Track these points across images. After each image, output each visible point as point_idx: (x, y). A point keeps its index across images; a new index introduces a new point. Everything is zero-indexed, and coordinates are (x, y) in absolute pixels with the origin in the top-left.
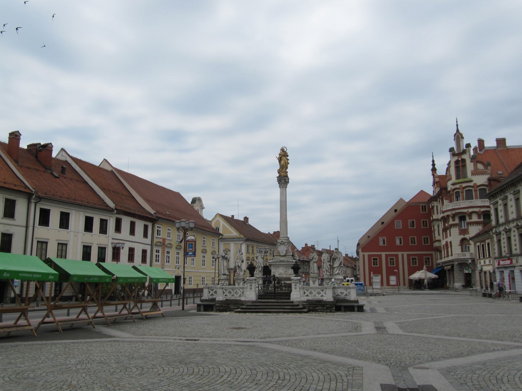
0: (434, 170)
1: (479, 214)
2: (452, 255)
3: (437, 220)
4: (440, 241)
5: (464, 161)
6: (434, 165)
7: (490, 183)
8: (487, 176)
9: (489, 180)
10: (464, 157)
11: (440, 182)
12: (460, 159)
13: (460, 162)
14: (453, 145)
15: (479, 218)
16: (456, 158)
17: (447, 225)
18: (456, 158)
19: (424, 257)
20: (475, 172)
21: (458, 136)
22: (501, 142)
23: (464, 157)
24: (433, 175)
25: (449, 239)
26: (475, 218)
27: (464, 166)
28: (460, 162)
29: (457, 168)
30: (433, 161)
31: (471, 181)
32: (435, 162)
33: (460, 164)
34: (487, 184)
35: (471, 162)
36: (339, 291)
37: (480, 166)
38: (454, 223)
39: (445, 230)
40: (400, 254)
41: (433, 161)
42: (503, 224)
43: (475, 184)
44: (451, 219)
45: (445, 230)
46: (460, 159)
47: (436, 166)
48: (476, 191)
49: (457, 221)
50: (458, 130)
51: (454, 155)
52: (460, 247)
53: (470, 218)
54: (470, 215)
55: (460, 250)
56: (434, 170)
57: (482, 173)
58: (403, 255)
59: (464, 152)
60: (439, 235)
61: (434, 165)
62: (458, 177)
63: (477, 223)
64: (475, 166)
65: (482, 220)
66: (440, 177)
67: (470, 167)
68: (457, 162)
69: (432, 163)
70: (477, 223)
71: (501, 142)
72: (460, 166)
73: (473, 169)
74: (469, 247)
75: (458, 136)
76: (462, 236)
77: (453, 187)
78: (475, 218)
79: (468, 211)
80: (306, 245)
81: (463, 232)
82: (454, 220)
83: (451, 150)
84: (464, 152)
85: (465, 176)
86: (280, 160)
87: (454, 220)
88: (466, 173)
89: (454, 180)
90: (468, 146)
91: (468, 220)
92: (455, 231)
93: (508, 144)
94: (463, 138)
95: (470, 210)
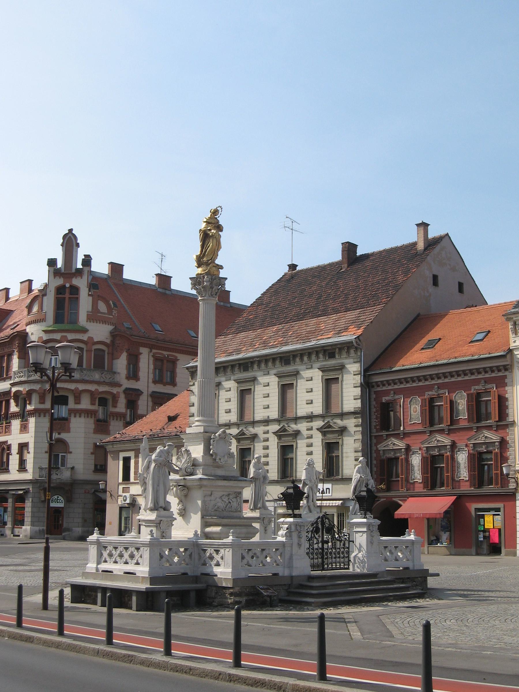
2: (22, 468)
5: (75, 290)
7: (113, 342)
8: (110, 328)
9: (113, 335)
10: (76, 282)
12: (68, 285)
13: (67, 291)
14: (59, 255)
15: (93, 404)
16: (60, 282)
18: (60, 282)
20: (94, 316)
21: (70, 242)
22: (116, 268)
23: (76, 282)
26: (85, 404)
28: (67, 291)
31: (84, 331)
33: (67, 295)
34: (108, 341)
35: (89, 295)
37: (102, 307)
38: (42, 406)
43: (91, 338)
46: (68, 285)
49: (48, 405)
52: (47, 455)
53: (78, 401)
54: (78, 396)
57: (104, 321)
63: (88, 413)
64: (95, 305)
67: (85, 302)
68: (60, 290)
70: (88, 413)
71: (116, 268)
73: (90, 309)
74: (63, 457)
75: (70, 242)
77: (45, 337)
78: (85, 404)
79: (77, 389)
83: (52, 263)
85: (75, 320)
86: (205, 237)
88: (77, 314)
91: (72, 404)
94: (78, 245)
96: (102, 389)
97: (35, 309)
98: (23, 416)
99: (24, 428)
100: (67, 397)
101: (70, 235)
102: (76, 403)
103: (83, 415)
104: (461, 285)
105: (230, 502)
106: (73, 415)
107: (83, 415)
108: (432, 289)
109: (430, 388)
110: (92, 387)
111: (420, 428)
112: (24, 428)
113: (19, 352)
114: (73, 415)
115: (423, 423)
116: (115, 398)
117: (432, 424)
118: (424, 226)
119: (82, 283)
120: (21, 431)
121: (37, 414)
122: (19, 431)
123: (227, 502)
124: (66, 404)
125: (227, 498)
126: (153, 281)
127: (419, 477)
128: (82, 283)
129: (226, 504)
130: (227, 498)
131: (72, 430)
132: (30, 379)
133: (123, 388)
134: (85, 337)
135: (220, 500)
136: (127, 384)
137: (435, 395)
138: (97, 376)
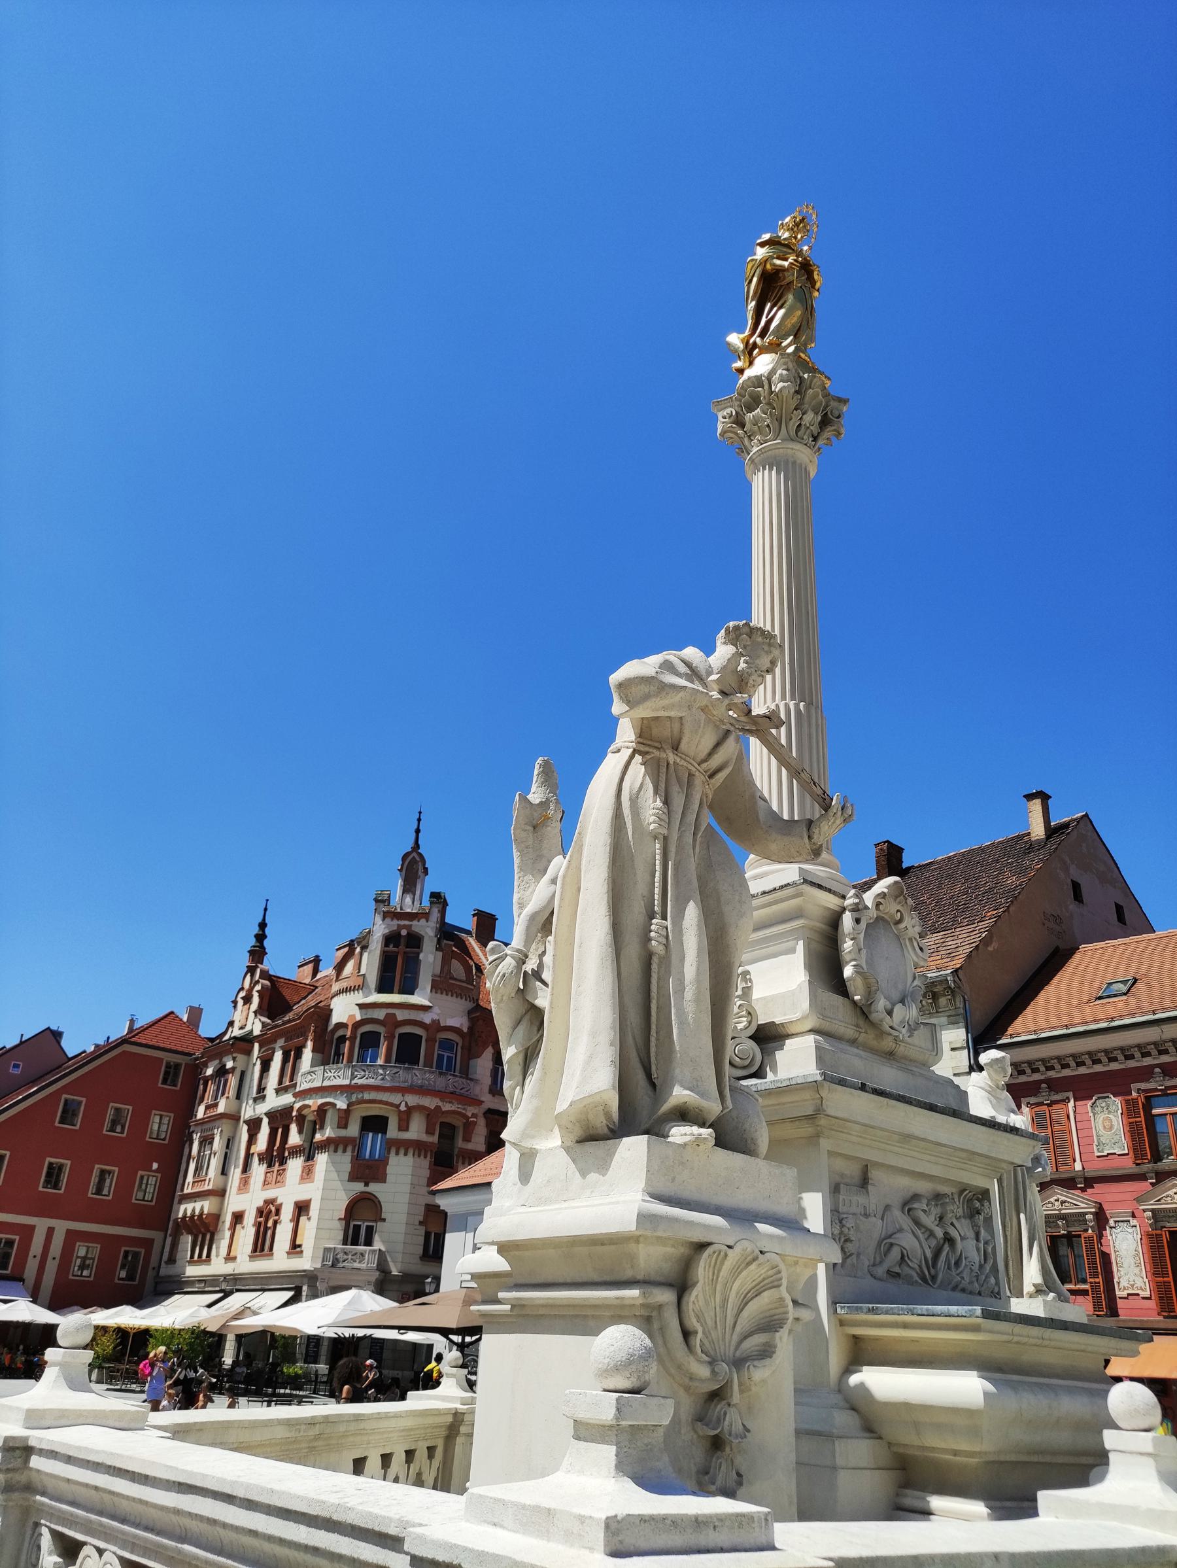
0: (258, 954)
1: (431, 1116)
5: (415, 941)
6: (261, 938)
12: (404, 932)
15: (429, 1132)
17: (294, 1138)
19: (143, 1251)
23: (419, 926)
24: (251, 970)
26: (416, 1130)
28: (403, 941)
30: (263, 925)
32: (267, 931)
38: (343, 1133)
40: (41, 1225)
41: (263, 925)
44: (331, 1118)
46: (404, 932)
47: (266, 943)
49: (353, 1130)
50: (417, 845)
53: (404, 1126)
55: (341, 1236)
56: (258, 954)
58: (51, 1231)
60: (224, 1172)
61: (261, 938)
63: (418, 1147)
64: (445, 963)
65: (434, 1139)
68: (390, 939)
69: (256, 930)
70: (418, 1147)
73: (438, 971)
76: (359, 1187)
78: (416, 1130)
91: (393, 1132)
95: (412, 1100)
96: (447, 1107)
97: (349, 967)
98: (309, 1152)
99: (307, 1173)
100: (387, 1118)
101: (414, 854)
102: (400, 1129)
103: (411, 1152)
104: (1119, 909)
105: (949, 1239)
106: (393, 1151)
107: (411, 1152)
108: (1073, 906)
109: (1145, 1074)
110: (430, 1102)
111: (1128, 1165)
112: (307, 1173)
113: (315, 1041)
114: (393, 1151)
115: (1137, 1151)
116: (469, 1127)
117: (1157, 1157)
119: (427, 930)
120: (302, 1178)
121: (332, 1148)
122: (298, 1178)
123: (939, 1233)
124: (384, 1132)
125: (936, 1211)
127: (1139, 1283)
129: (933, 1243)
130: (936, 1211)
131: (390, 1178)
132: (326, 1083)
133: (485, 1107)
134: (427, 1018)
135: (905, 1221)
136: (489, 1102)
137: (1156, 1090)
138: (440, 1083)
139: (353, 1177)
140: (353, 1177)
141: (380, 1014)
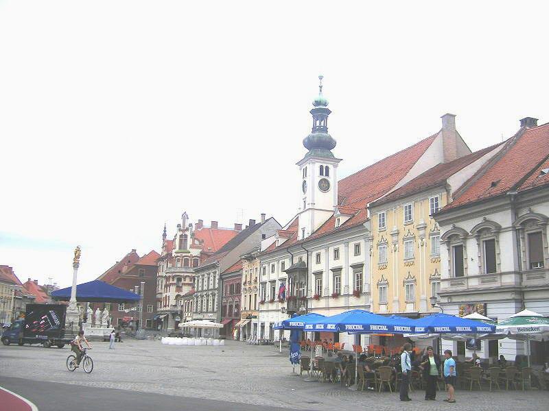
0: (165, 235)
3: (162, 276)
4: (161, 293)
5: (186, 236)
6: (165, 231)
8: (200, 250)
9: (201, 253)
11: (168, 245)
15: (191, 281)
16: (181, 233)
18: (181, 233)
21: (185, 216)
22: (215, 224)
25: (168, 294)
26: (188, 281)
27: (186, 240)
29: (181, 241)
30: (165, 228)
36: (105, 331)
39: (166, 286)
41: (165, 228)
42: (200, 292)
45: (166, 286)
48: (191, 260)
49: (175, 281)
51: (180, 230)
56: (165, 235)
57: (197, 248)
59: (187, 229)
61: (165, 231)
62: (180, 248)
63: (189, 284)
64: (193, 242)
66: (168, 241)
67: (189, 241)
68: (181, 236)
70: (189, 284)
71: (215, 224)
72: (183, 239)
75: (185, 216)
78: (188, 281)
80: (29, 279)
81: (179, 288)
82: (173, 281)
83: (179, 226)
84: (187, 229)
85: (185, 248)
87: (173, 281)
89: (177, 249)
90: (191, 225)
91: (183, 281)
92: (173, 288)
93: (220, 226)
94: (188, 218)
110: (190, 275)
118: (263, 215)
126: (233, 227)
128: (188, 233)
139: (177, 291)
140: (177, 291)
141: (179, 255)
